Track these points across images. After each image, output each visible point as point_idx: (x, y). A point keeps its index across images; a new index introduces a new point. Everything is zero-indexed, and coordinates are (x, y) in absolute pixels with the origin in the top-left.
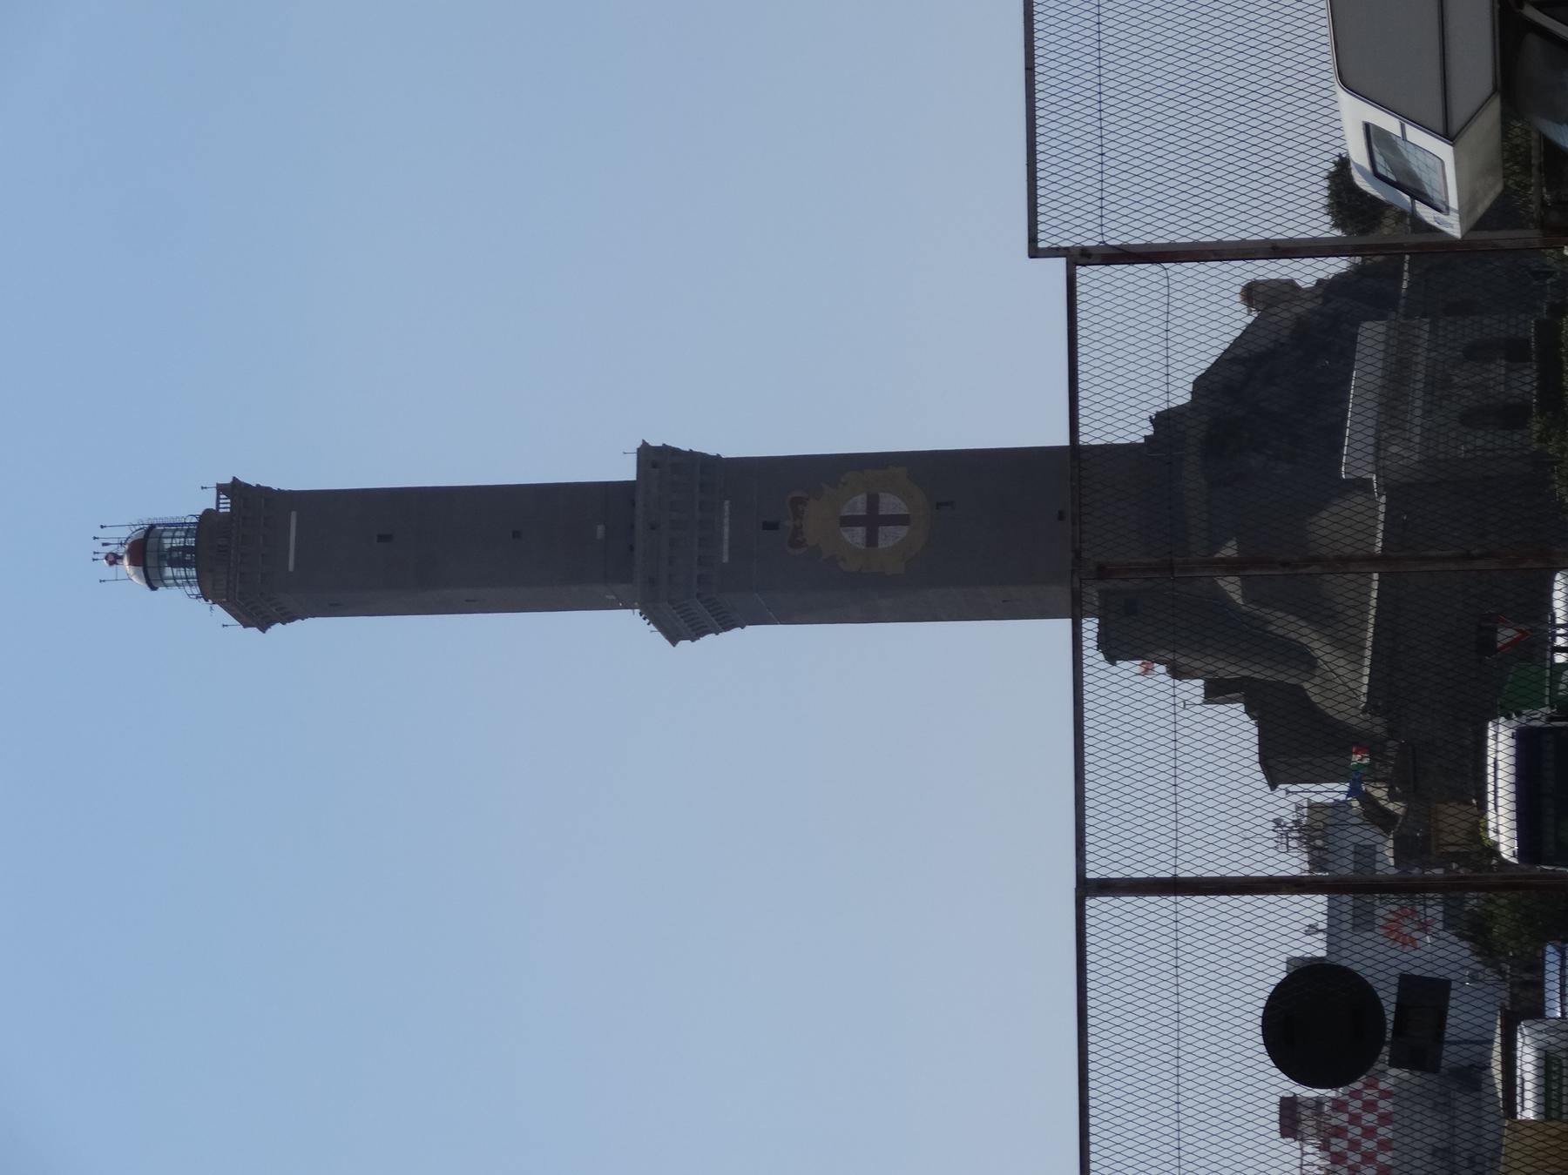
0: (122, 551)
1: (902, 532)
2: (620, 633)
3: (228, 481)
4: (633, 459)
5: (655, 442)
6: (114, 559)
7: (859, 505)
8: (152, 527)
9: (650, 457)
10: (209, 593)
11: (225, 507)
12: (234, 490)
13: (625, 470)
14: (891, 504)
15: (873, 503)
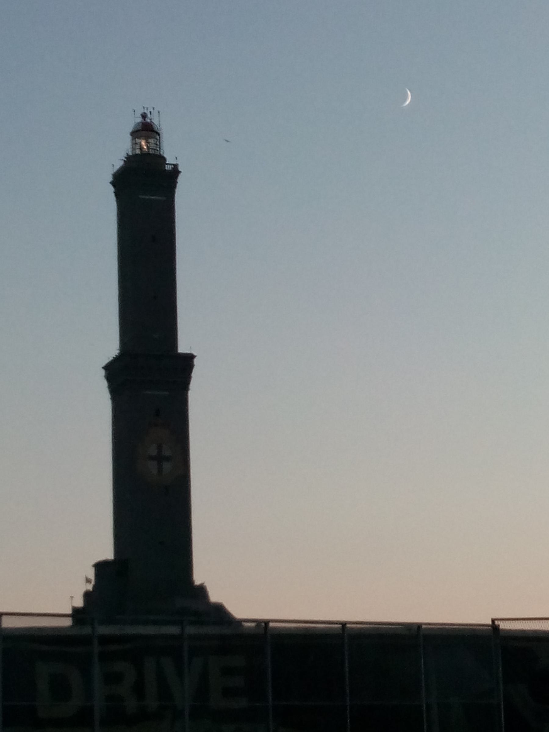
0: (148, 121)
1: (155, 472)
2: (109, 345)
3: (180, 169)
4: (188, 352)
5: (196, 361)
6: (144, 116)
7: (167, 452)
8: (159, 134)
9: (189, 359)
10: (130, 160)
11: (168, 168)
12: (175, 172)
13: (182, 348)
14: (167, 466)
15: (168, 459)
